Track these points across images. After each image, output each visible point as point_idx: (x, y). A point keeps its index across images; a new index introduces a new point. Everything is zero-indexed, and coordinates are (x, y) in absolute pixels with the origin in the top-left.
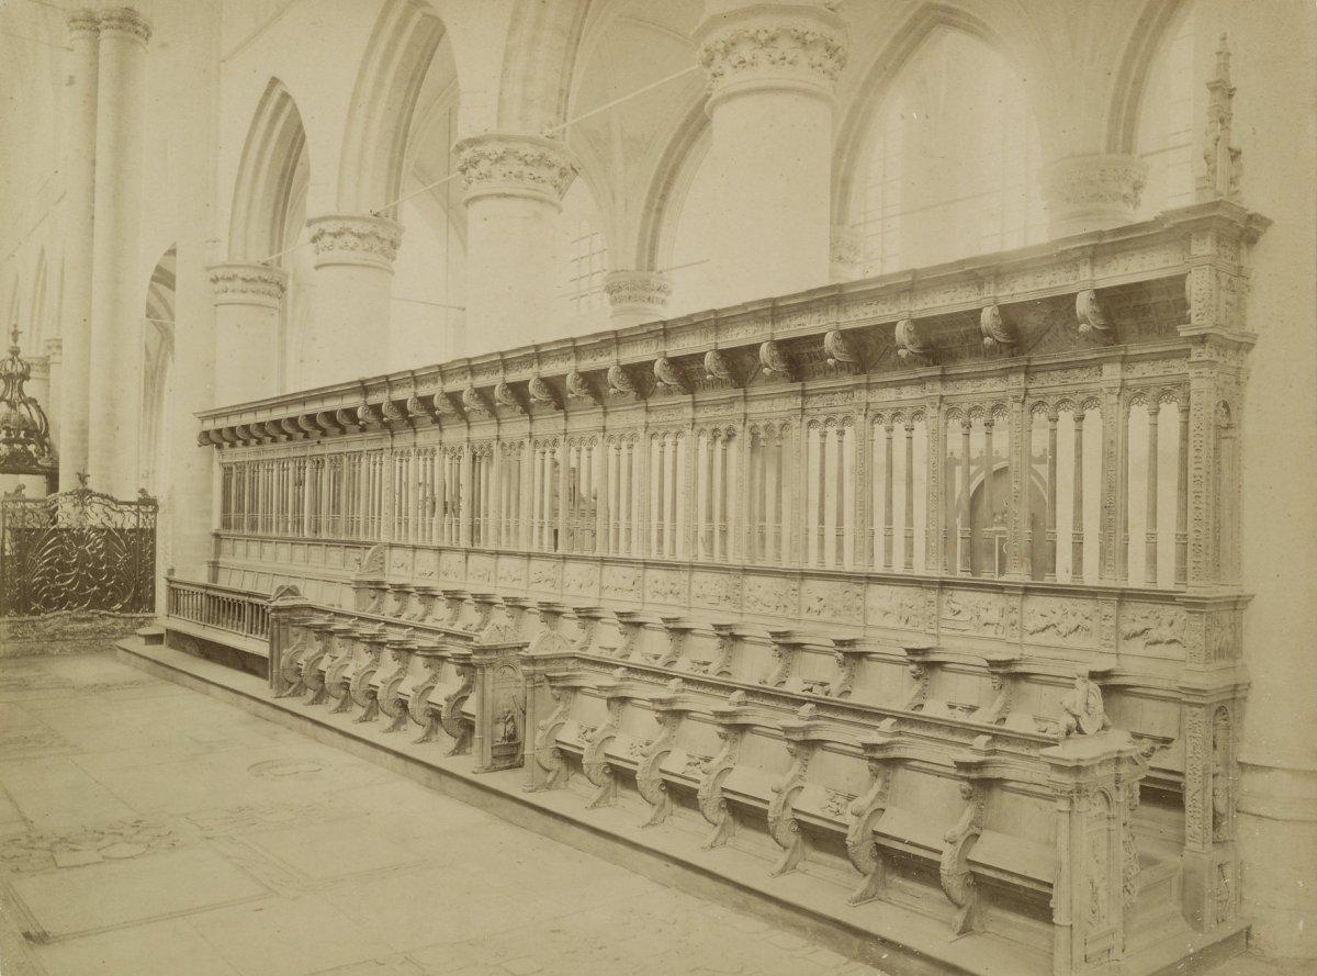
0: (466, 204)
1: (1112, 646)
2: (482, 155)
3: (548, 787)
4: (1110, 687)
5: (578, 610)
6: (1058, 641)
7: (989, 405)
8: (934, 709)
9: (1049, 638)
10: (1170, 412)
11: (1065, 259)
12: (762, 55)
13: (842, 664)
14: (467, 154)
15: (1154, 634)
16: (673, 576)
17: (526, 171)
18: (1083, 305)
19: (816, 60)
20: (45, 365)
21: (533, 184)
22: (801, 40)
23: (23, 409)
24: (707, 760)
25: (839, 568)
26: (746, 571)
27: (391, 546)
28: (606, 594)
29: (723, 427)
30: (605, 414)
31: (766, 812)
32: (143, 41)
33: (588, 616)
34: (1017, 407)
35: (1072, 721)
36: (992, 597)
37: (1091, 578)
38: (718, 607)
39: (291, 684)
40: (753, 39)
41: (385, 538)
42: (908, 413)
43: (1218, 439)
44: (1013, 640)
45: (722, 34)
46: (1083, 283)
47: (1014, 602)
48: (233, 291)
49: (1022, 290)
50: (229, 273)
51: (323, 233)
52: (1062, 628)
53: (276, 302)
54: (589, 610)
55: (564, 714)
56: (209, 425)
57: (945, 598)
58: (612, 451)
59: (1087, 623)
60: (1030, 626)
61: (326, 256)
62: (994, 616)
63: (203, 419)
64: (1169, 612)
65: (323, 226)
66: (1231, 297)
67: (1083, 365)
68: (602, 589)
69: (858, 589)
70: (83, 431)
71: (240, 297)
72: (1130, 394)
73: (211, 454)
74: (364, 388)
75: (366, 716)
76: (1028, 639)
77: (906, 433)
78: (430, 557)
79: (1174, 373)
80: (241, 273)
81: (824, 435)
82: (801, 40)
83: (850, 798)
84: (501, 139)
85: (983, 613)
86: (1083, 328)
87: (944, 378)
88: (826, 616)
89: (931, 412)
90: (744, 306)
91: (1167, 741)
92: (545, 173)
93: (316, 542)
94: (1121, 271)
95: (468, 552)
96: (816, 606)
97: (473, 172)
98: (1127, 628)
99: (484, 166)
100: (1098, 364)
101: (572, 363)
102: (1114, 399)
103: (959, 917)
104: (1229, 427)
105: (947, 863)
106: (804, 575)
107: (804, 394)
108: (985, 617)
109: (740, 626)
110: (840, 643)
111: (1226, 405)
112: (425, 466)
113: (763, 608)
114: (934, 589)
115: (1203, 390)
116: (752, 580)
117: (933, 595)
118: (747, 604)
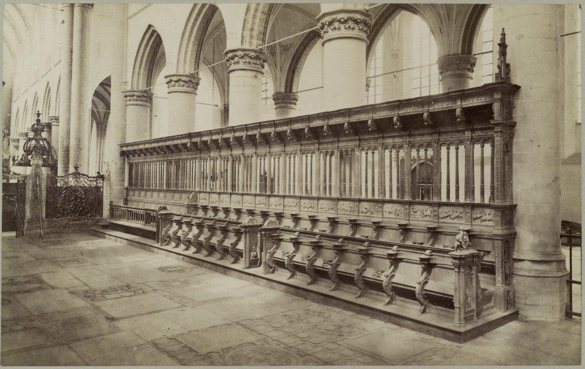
0: (229, 72)
2: (236, 56)
3: (273, 272)
4: (471, 235)
5: (276, 214)
6: (451, 221)
7: (425, 144)
8: (409, 243)
9: (448, 220)
10: (488, 147)
12: (342, 26)
13: (375, 230)
14: (230, 55)
15: (484, 218)
16: (311, 201)
17: (252, 61)
18: (458, 112)
19: (361, 28)
20: (49, 126)
21: (254, 66)
22: (356, 21)
23: (41, 143)
24: (331, 261)
25: (373, 198)
26: (338, 200)
27: (200, 192)
28: (285, 208)
29: (330, 151)
30: (285, 146)
31: (354, 278)
32: (91, 7)
33: (280, 216)
34: (435, 145)
35: (459, 243)
36: (428, 207)
37: (462, 200)
39: (166, 241)
40: (339, 21)
41: (197, 189)
42: (397, 146)
43: (504, 155)
44: (435, 221)
45: (328, 19)
46: (458, 106)
47: (436, 208)
48: (133, 100)
49: (438, 107)
50: (131, 94)
51: (171, 81)
52: (452, 217)
53: (149, 104)
54: (280, 213)
55: (277, 248)
56: (124, 149)
57: (411, 208)
58: (272, 159)
59: (461, 215)
60: (441, 216)
61: (172, 89)
62: (429, 213)
63: (122, 147)
64: (488, 211)
65: (172, 78)
66: (507, 111)
67: (458, 131)
68: (284, 206)
69: (380, 205)
70: (67, 151)
71: (135, 102)
72: (474, 141)
73: (124, 160)
74: (190, 136)
75: (197, 251)
76: (440, 220)
78: (216, 196)
80: (136, 94)
81: (367, 154)
82: (356, 21)
83: (383, 272)
84: (243, 50)
85: (425, 212)
86: (458, 120)
87: (410, 135)
88: (369, 214)
89: (406, 146)
90: (339, 111)
91: (489, 252)
92: (258, 62)
93: (167, 191)
95: (231, 194)
97: (233, 61)
98: (474, 216)
99: (236, 59)
100: (463, 132)
101: (273, 129)
102: (469, 142)
103: (422, 308)
104: (508, 151)
105: (417, 290)
106: (360, 201)
107: (360, 140)
108: (426, 213)
109: (337, 218)
110: (374, 223)
111: (506, 145)
112: (224, 163)
113: (345, 212)
115: (498, 139)
116: (341, 203)
117: (407, 207)
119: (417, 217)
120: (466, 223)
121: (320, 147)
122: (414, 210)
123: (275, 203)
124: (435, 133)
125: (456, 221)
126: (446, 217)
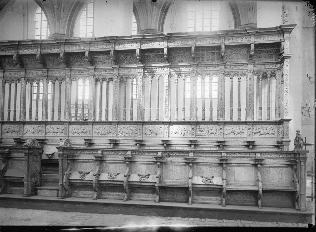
1: (251, 136)
9: (232, 135)
11: (219, 36)
15: (262, 132)
28: (48, 135)
38: (105, 136)
44: (221, 137)
47: (221, 127)
54: (43, 140)
57: (197, 127)
59: (243, 131)
62: (214, 131)
67: (242, 65)
68: (46, 133)
77: (230, 80)
79: (267, 68)
94: (262, 40)
96: (149, 133)
98: (254, 131)
108: (211, 131)
114: (194, 125)
117: (194, 127)
118: (119, 134)
119: (203, 135)
120: (113, 136)
121: (95, 73)
122: (201, 129)
123: (32, 131)
124: (222, 65)
125: (239, 136)
126: (230, 134)
